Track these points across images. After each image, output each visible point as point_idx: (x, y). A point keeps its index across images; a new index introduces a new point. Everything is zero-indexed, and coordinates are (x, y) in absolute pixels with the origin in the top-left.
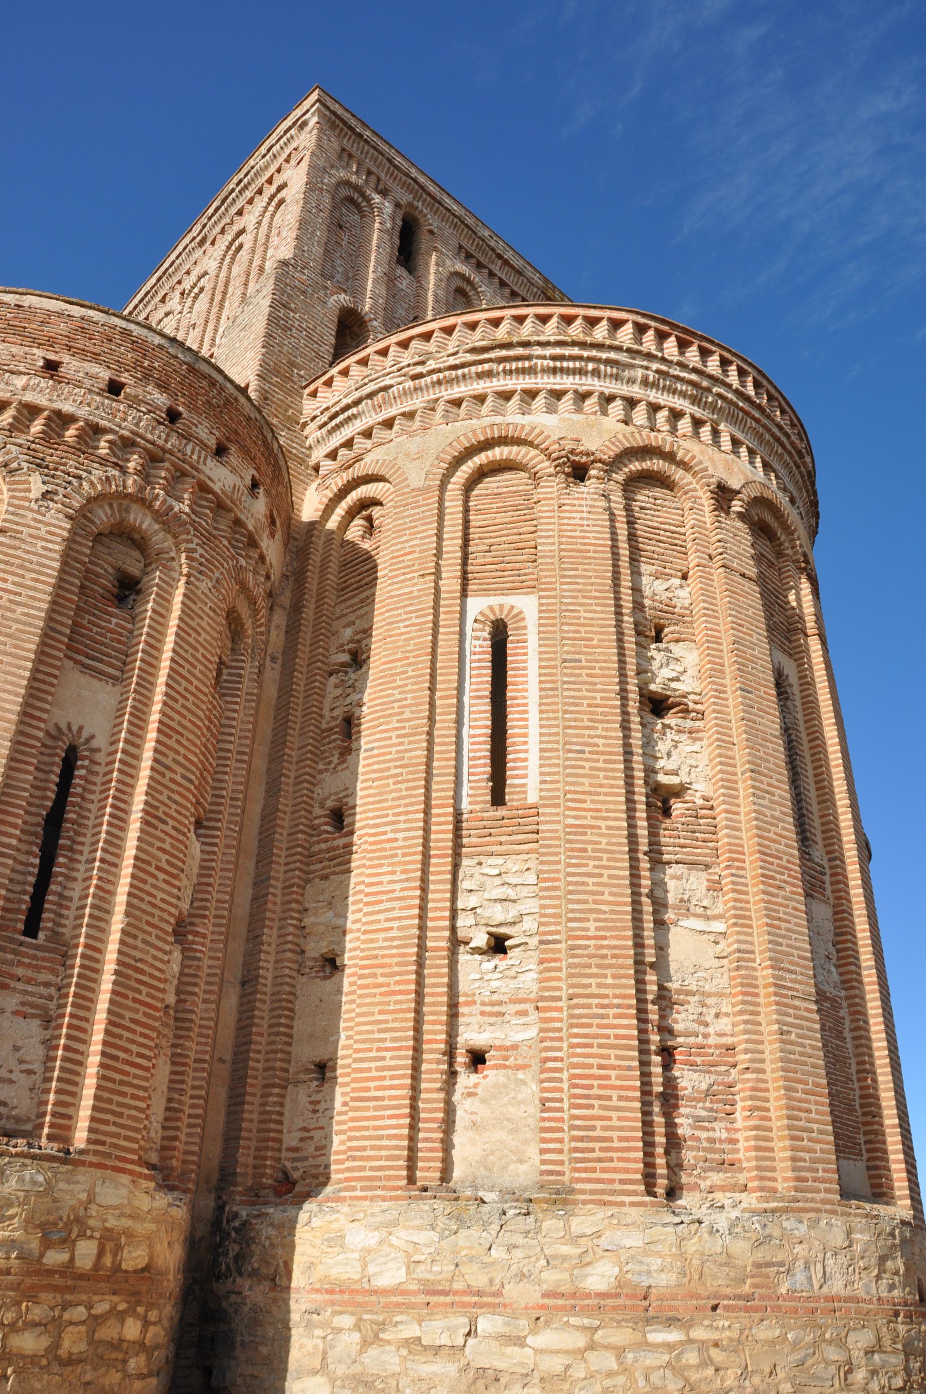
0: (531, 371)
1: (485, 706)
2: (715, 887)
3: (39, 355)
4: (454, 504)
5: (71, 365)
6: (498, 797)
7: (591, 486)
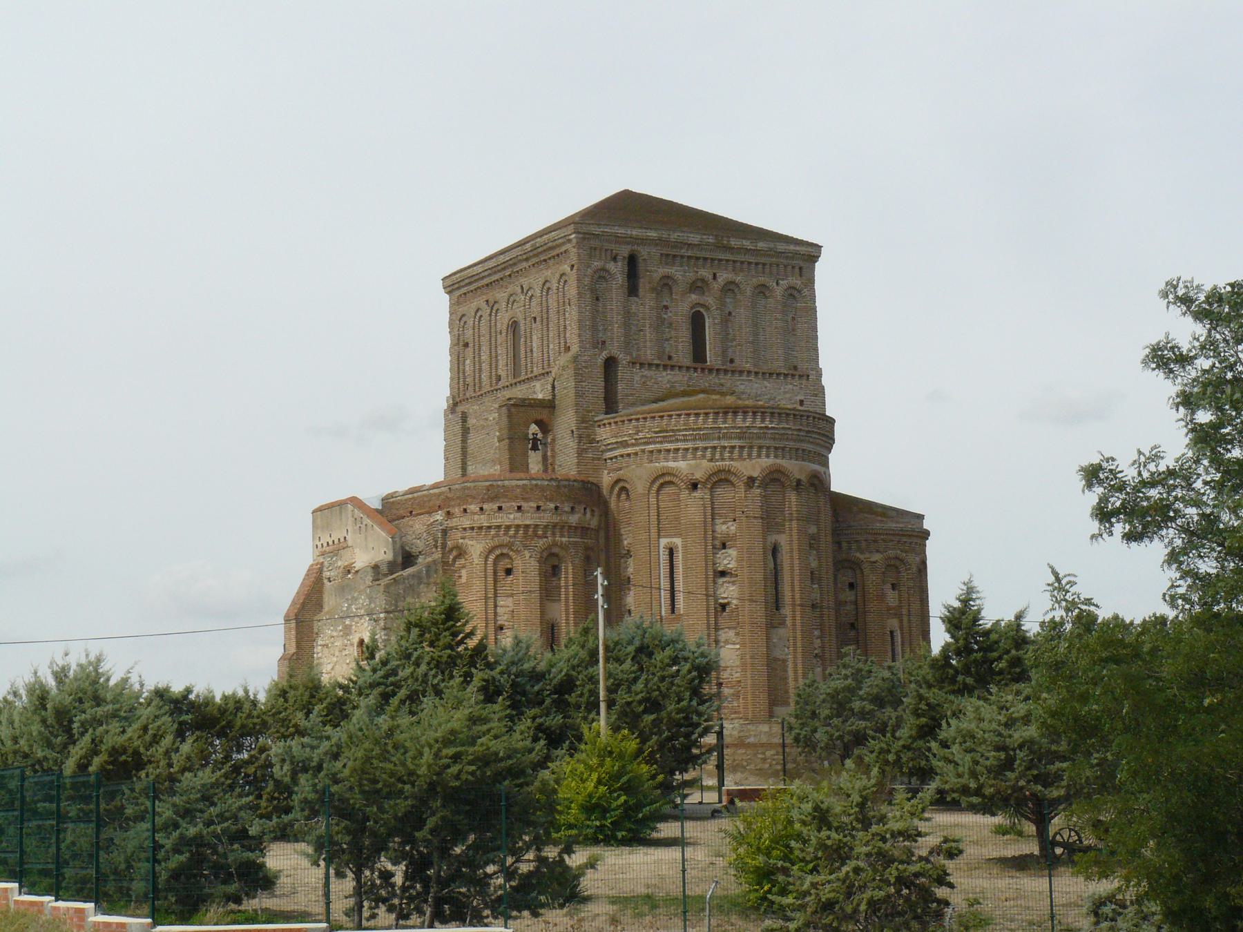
0: (677, 440)
1: (668, 580)
2: (737, 634)
3: (515, 504)
4: (653, 500)
5: (525, 505)
6: (673, 612)
7: (698, 494)
